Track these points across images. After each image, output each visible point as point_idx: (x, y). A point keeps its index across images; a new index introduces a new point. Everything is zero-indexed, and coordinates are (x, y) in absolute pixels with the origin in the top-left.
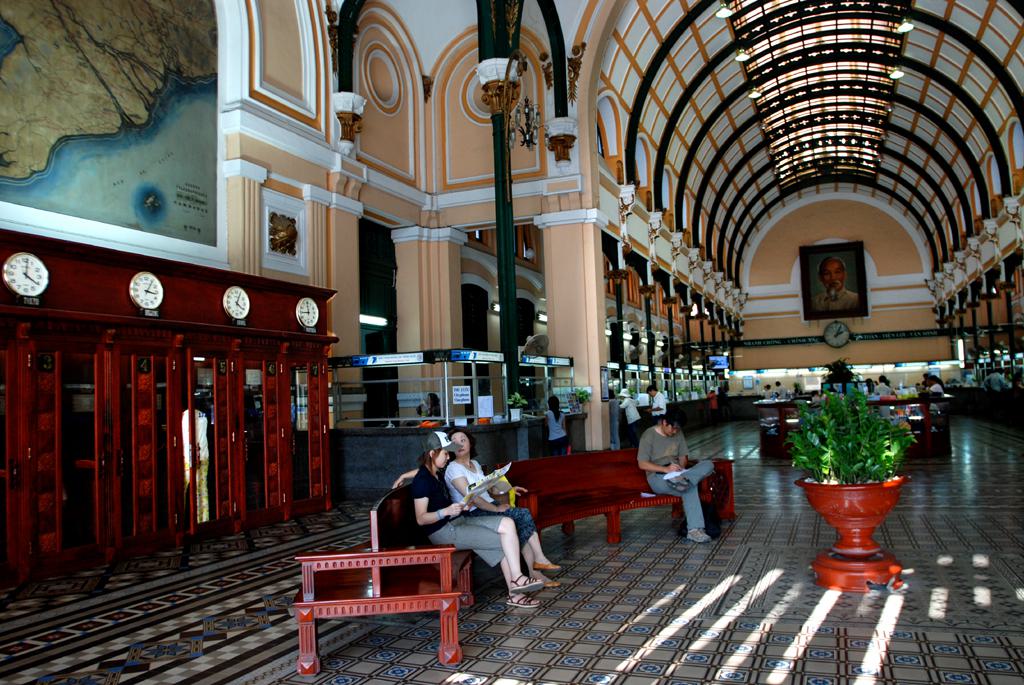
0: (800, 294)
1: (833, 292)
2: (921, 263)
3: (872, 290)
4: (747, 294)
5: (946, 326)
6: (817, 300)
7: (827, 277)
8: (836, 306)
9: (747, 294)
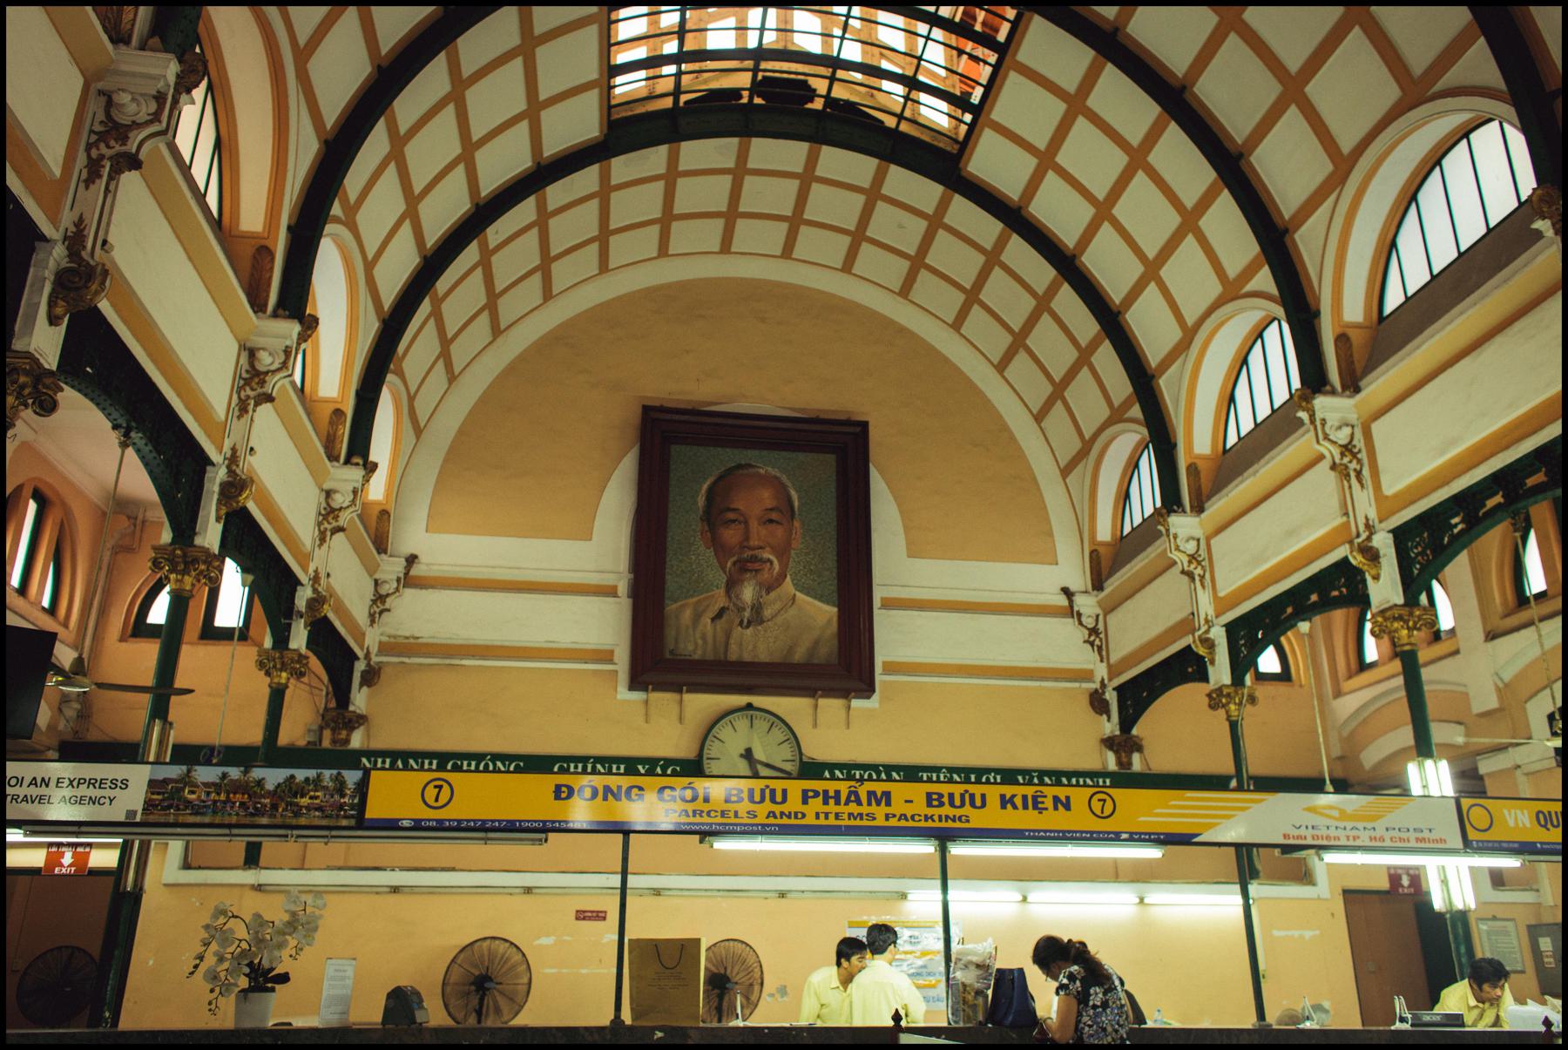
0: (623, 588)
1: (748, 593)
2: (1050, 534)
3: (889, 604)
4: (412, 560)
5: (1137, 763)
6: (687, 614)
7: (731, 535)
8: (756, 645)
9: (412, 560)
